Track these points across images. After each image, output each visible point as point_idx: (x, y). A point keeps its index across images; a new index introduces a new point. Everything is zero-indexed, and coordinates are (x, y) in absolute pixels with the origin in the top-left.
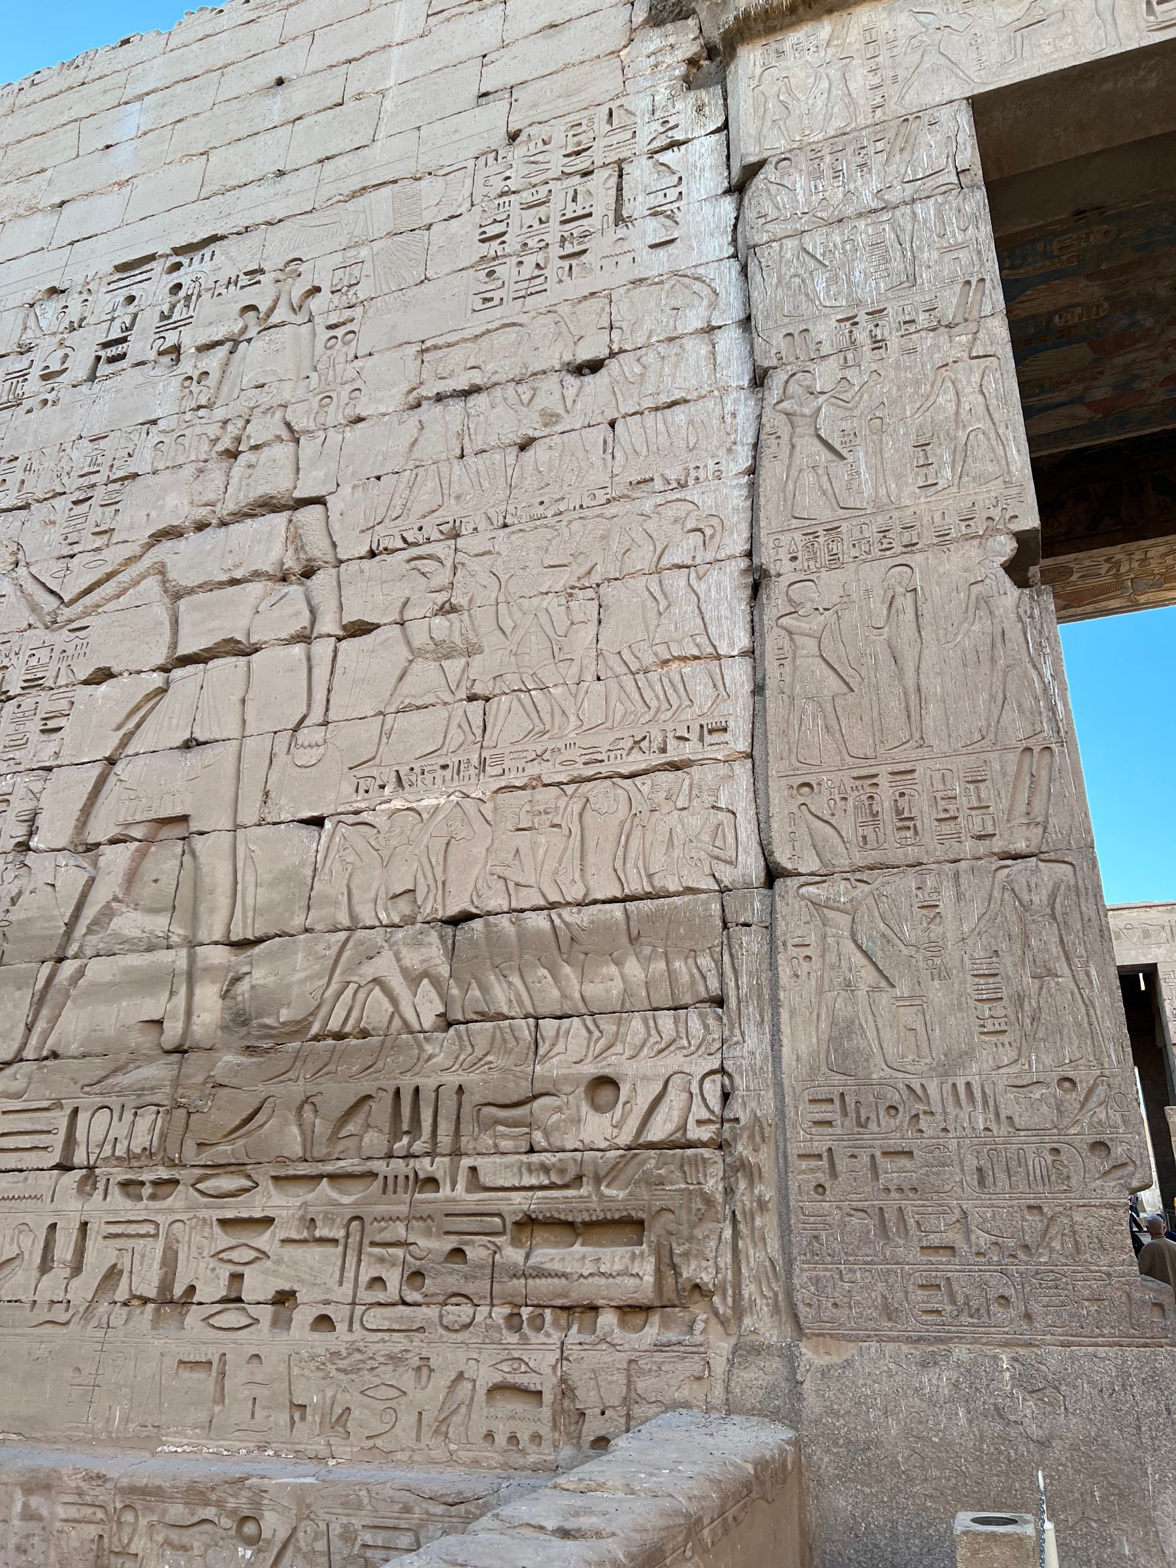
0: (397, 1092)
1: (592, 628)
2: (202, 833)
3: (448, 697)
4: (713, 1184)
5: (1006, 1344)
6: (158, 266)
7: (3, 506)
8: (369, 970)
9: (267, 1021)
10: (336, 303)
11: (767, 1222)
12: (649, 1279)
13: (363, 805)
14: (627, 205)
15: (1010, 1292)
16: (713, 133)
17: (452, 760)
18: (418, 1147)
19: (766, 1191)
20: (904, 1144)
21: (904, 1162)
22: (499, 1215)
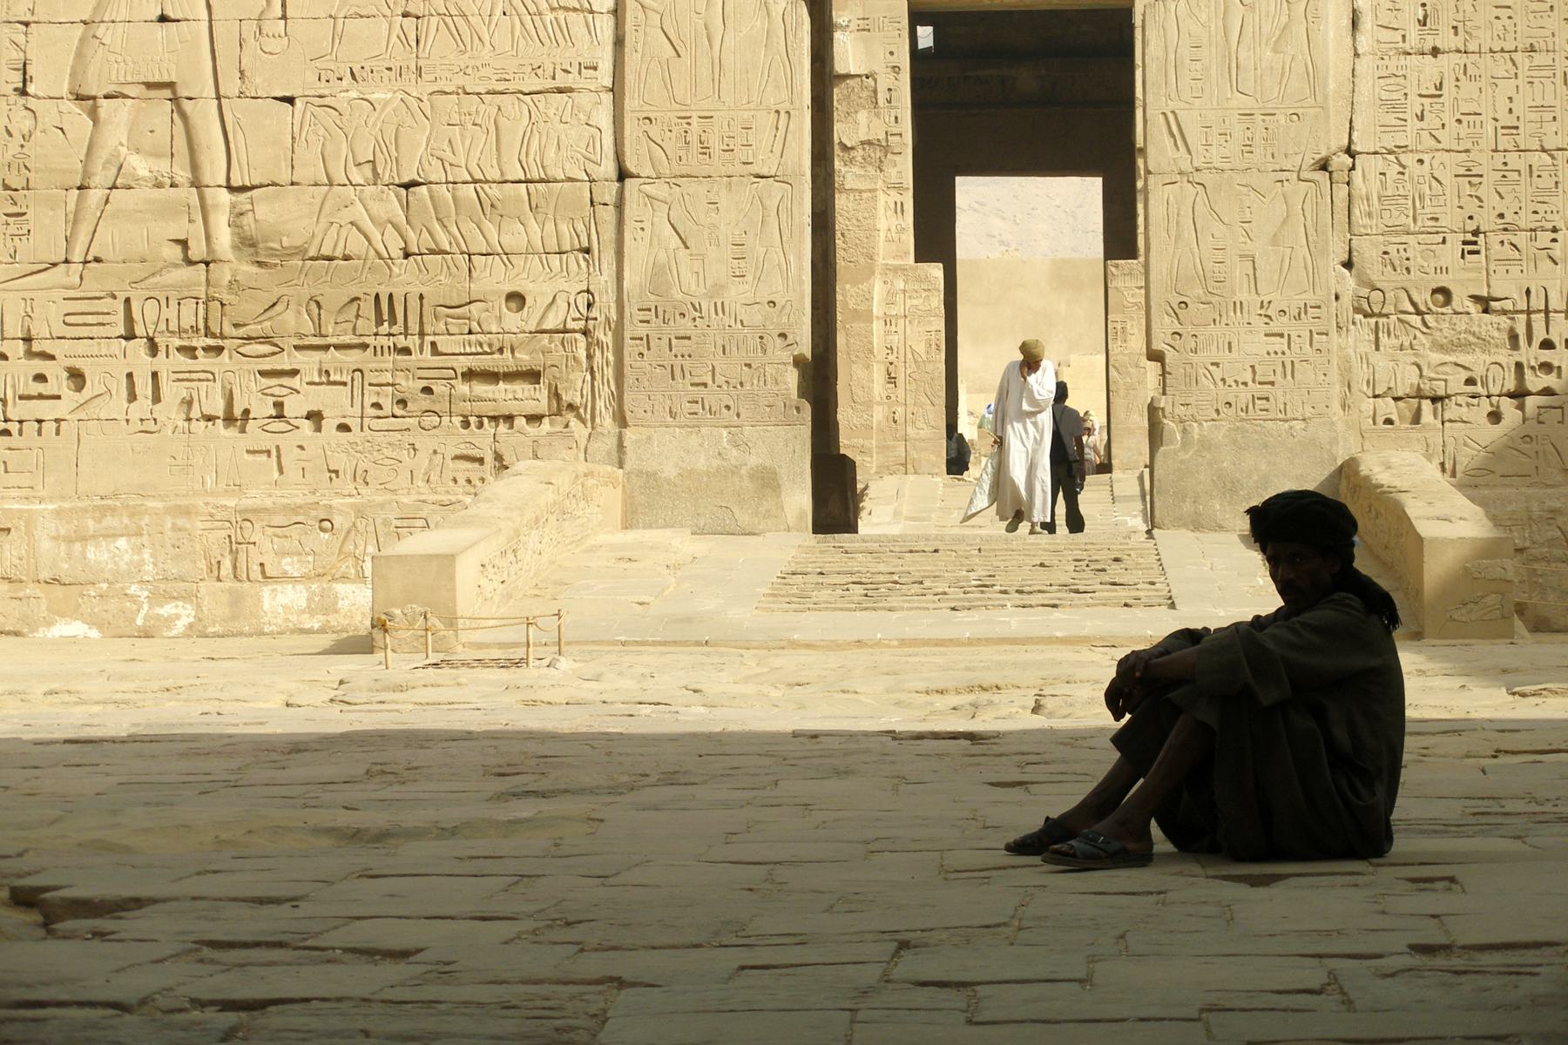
0: (377, 296)
2: (190, 99)
3: (388, 12)
4: (582, 354)
5: (726, 427)
8: (346, 216)
9: (272, 245)
11: (609, 372)
12: (545, 402)
13: (326, 92)
15: (731, 403)
17: (395, 65)
18: (395, 330)
19: (611, 358)
20: (688, 333)
21: (686, 342)
22: (453, 369)
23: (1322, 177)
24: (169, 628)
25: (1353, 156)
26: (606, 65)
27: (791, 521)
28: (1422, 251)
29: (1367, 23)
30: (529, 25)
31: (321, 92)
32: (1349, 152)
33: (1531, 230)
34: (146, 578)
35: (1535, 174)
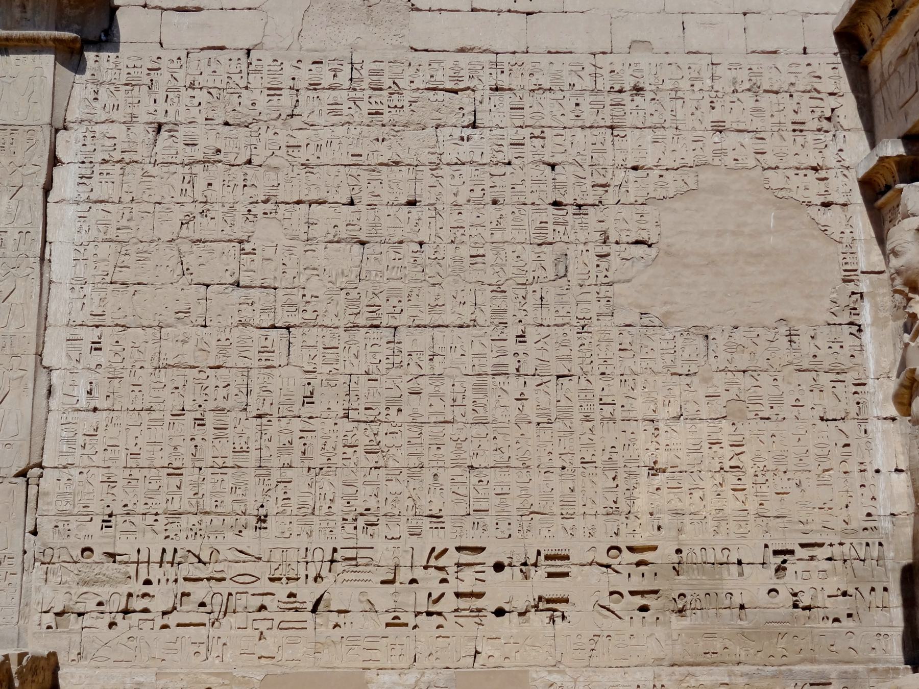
23: (21, 480)
28: (78, 526)
32: (40, 466)
33: (143, 514)
35: (148, 480)
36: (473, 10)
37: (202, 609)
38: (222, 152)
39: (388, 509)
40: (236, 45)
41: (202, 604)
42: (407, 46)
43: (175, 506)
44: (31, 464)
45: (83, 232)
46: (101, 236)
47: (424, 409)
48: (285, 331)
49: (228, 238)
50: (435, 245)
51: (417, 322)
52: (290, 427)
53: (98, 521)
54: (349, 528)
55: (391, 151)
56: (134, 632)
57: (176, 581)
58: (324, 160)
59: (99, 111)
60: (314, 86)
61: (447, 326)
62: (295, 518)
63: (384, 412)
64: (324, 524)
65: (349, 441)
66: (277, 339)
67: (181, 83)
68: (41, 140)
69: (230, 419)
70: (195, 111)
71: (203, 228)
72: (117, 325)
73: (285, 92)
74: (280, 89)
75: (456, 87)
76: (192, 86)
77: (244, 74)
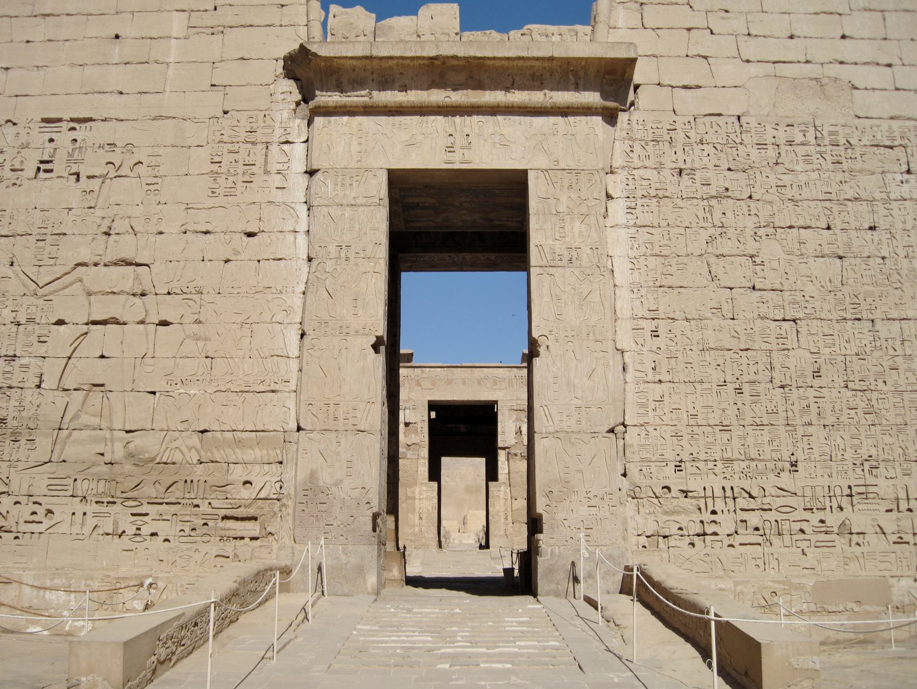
1: (248, 340)
4: (276, 509)
6: (65, 126)
7: (3, 234)
8: (175, 444)
10: (150, 173)
11: (290, 518)
12: (258, 531)
13: (170, 390)
14: (269, 165)
15: (344, 534)
16: (304, 142)
19: (291, 511)
23: (611, 435)
24: (81, 632)
25: (625, 426)
26: (294, 381)
27: (370, 590)
29: (630, 369)
30: (260, 363)
31: (167, 390)
34: (71, 608)
36: (897, 89)
37: (756, 532)
38: (730, 189)
39: (886, 456)
40: (730, 113)
41: (757, 529)
42: (852, 113)
43: (729, 455)
44: (617, 423)
45: (635, 249)
46: (649, 252)
47: (902, 381)
48: (792, 323)
49: (743, 253)
50: (894, 260)
51: (889, 317)
52: (807, 394)
53: (671, 466)
54: (859, 471)
55: (852, 190)
56: (708, 550)
57: (735, 511)
58: (804, 196)
59: (636, 160)
60: (790, 143)
61: (910, 319)
62: (818, 464)
63: (873, 383)
64: (840, 468)
65: (851, 405)
66: (788, 329)
67: (693, 140)
68: (599, 180)
69: (761, 388)
70: (706, 160)
71: (726, 246)
72: (669, 318)
73: (770, 147)
74: (766, 144)
75: (892, 144)
76: (701, 142)
77: (738, 134)
